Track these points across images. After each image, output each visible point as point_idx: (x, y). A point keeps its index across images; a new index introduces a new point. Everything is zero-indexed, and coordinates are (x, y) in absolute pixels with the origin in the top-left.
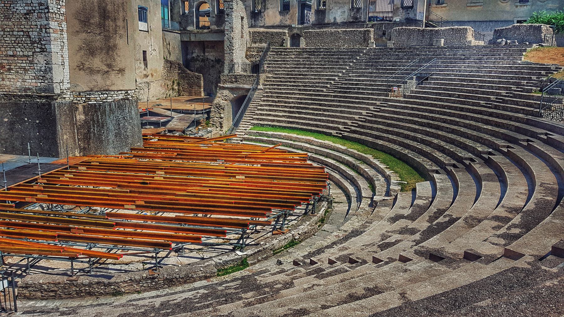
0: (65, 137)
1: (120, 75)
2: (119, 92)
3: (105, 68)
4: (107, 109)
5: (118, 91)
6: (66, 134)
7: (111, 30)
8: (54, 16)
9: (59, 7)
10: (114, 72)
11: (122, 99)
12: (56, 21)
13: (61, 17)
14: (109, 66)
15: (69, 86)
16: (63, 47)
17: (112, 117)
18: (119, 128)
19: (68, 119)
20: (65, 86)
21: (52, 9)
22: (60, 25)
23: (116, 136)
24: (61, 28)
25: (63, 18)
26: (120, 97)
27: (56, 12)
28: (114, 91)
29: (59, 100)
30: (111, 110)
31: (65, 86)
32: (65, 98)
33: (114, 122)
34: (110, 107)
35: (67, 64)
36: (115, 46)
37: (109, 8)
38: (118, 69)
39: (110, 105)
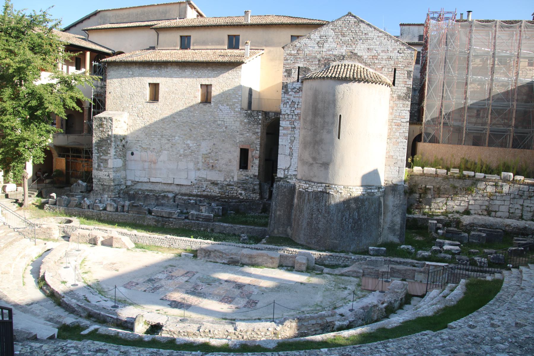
0: (278, 213)
1: (322, 169)
2: (319, 185)
3: (311, 161)
4: (306, 198)
5: (318, 183)
6: (280, 211)
7: (319, 126)
8: (286, 116)
9: (293, 109)
10: (317, 165)
11: (320, 191)
12: (287, 120)
13: (294, 117)
14: (314, 159)
15: (295, 173)
16: (292, 142)
17: (308, 206)
18: (312, 218)
19: (286, 199)
20: (290, 173)
21: (285, 111)
22: (292, 123)
23: (308, 225)
24: (293, 126)
25: (297, 118)
26: (319, 190)
27: (289, 113)
28: (314, 183)
29: (281, 182)
30: (308, 199)
31: (290, 173)
32: (288, 182)
33: (309, 211)
34: (309, 196)
35: (295, 155)
36: (321, 141)
37: (320, 106)
38: (321, 162)
39: (309, 194)
